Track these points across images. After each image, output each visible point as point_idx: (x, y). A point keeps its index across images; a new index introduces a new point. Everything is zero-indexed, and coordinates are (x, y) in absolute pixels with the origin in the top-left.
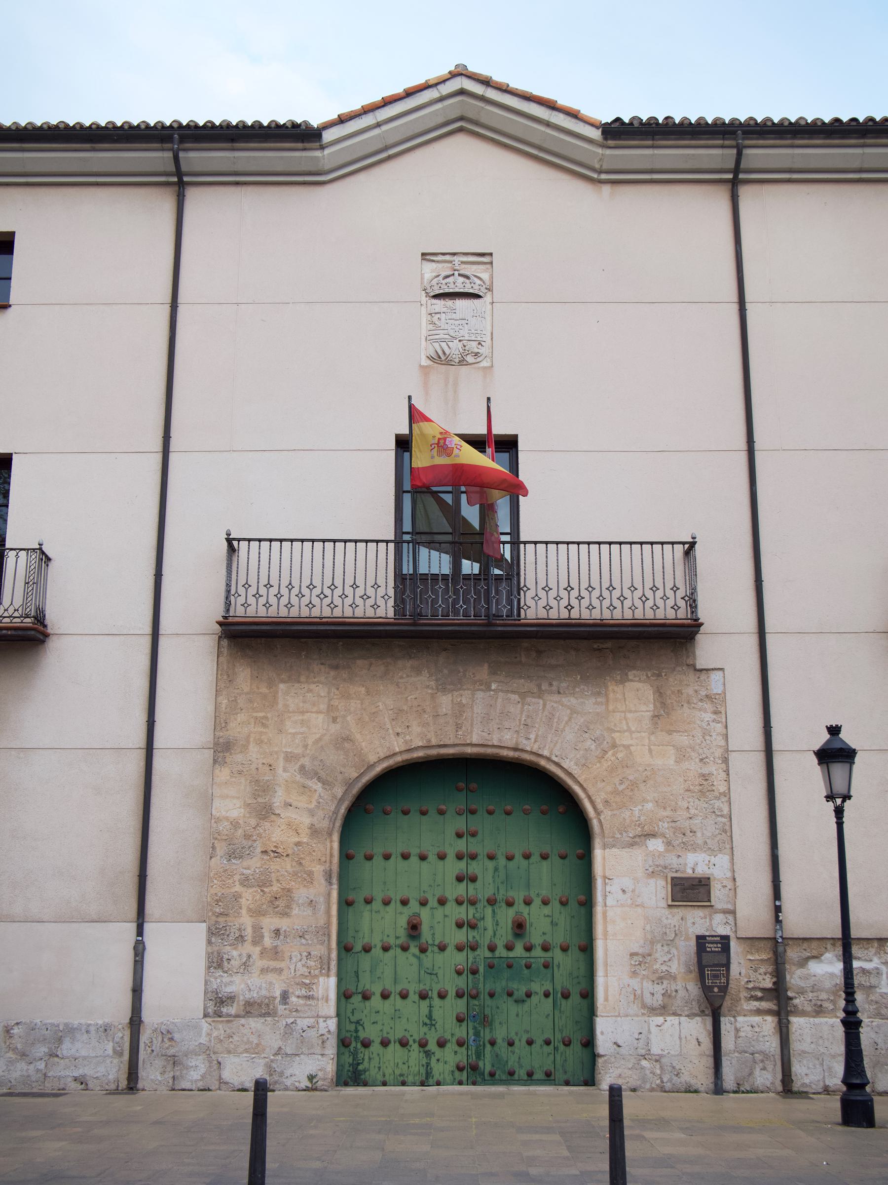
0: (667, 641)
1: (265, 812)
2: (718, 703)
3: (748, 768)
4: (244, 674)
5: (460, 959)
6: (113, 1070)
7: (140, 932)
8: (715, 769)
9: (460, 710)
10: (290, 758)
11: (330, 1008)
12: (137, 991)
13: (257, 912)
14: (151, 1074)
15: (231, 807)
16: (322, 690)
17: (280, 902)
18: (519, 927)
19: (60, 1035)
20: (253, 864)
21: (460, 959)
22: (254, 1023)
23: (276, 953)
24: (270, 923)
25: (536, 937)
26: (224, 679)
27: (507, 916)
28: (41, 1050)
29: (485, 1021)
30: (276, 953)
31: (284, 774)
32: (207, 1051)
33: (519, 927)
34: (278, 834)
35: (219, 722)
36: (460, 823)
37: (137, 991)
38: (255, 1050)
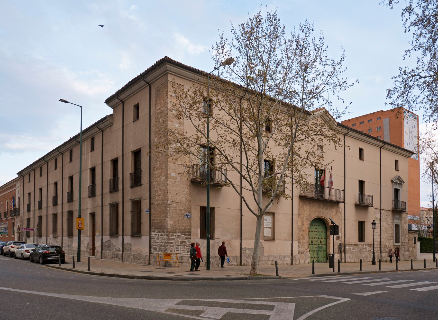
0: (335, 204)
1: (303, 225)
2: (341, 212)
3: (343, 221)
4: (301, 203)
5: (316, 246)
6: (290, 262)
7: (292, 242)
8: (340, 221)
9: (320, 211)
10: (305, 217)
11: (309, 253)
12: (292, 251)
13: (302, 239)
14: (294, 262)
15: (300, 224)
16: (308, 207)
17: (304, 238)
18: (321, 242)
19: (285, 257)
20: (302, 232)
21: (316, 246)
22: (303, 255)
23: (304, 245)
24: (303, 241)
25: (322, 243)
26: (299, 204)
27: (320, 240)
28: (283, 259)
29: (318, 254)
30: (304, 245)
31: (305, 219)
32: (299, 259)
33: (321, 242)
34: (304, 228)
35: (299, 211)
36: (316, 227)
37: (292, 251)
38: (303, 259)
